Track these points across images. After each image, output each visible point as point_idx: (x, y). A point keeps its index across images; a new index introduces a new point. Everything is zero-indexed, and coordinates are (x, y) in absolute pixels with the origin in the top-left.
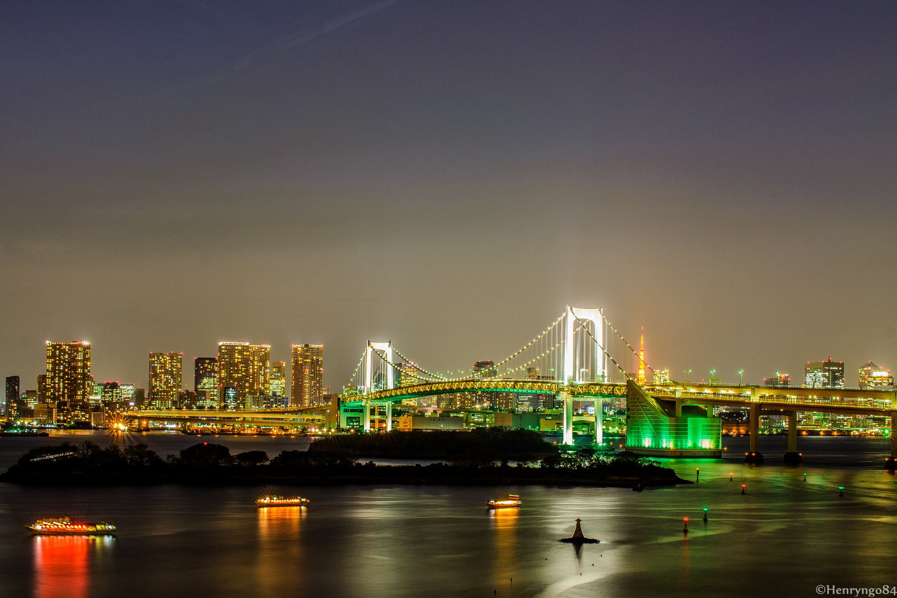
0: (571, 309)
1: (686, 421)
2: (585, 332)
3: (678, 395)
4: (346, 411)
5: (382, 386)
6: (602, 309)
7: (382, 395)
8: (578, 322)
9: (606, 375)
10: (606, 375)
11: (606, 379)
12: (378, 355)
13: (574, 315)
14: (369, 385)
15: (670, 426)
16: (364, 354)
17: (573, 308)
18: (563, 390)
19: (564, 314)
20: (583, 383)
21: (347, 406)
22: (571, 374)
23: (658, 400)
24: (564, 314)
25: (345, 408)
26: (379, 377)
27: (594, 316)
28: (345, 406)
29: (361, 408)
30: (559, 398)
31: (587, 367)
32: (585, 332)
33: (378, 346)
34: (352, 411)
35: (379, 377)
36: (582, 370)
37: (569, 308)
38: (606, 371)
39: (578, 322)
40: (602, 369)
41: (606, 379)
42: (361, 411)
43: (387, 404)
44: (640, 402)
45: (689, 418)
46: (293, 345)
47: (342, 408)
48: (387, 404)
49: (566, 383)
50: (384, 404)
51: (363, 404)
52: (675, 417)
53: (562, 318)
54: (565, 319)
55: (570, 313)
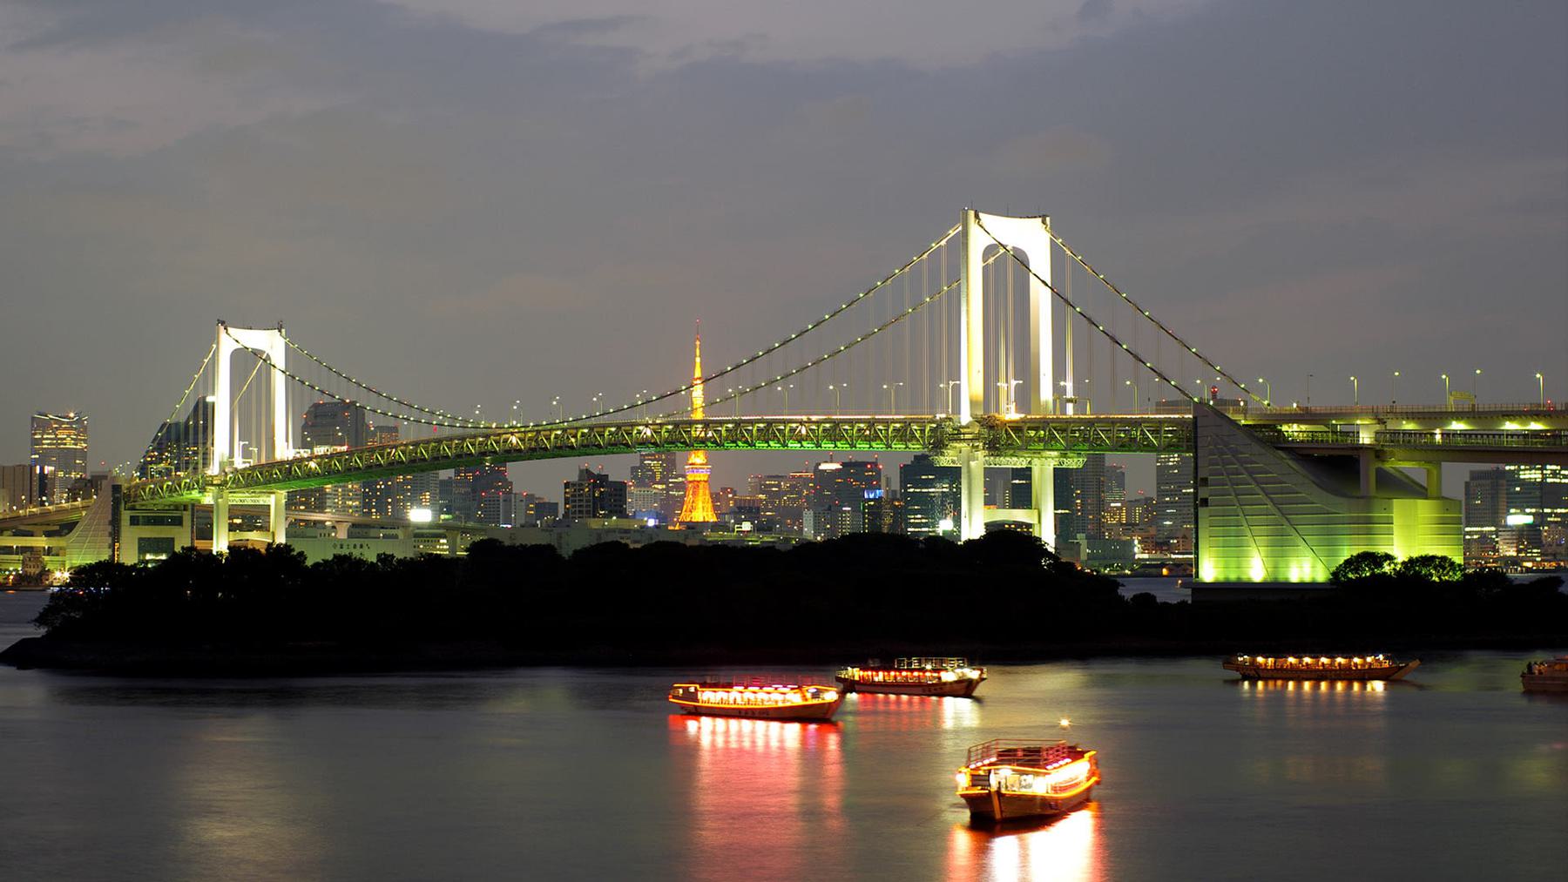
0: (977, 216)
1: (1389, 509)
4: (134, 521)
5: (256, 449)
6: (1048, 219)
7: (266, 474)
9: (1070, 394)
10: (1070, 394)
11: (1070, 407)
16: (206, 361)
17: (981, 215)
18: (957, 435)
19: (952, 233)
21: (138, 507)
25: (134, 513)
28: (133, 509)
29: (177, 514)
30: (946, 460)
37: (972, 213)
38: (1069, 385)
41: (1070, 407)
42: (178, 522)
43: (270, 500)
44: (1242, 462)
45: (1395, 500)
47: (126, 516)
48: (270, 500)
49: (965, 418)
50: (263, 500)
51: (207, 499)
52: (1362, 497)
53: (943, 243)
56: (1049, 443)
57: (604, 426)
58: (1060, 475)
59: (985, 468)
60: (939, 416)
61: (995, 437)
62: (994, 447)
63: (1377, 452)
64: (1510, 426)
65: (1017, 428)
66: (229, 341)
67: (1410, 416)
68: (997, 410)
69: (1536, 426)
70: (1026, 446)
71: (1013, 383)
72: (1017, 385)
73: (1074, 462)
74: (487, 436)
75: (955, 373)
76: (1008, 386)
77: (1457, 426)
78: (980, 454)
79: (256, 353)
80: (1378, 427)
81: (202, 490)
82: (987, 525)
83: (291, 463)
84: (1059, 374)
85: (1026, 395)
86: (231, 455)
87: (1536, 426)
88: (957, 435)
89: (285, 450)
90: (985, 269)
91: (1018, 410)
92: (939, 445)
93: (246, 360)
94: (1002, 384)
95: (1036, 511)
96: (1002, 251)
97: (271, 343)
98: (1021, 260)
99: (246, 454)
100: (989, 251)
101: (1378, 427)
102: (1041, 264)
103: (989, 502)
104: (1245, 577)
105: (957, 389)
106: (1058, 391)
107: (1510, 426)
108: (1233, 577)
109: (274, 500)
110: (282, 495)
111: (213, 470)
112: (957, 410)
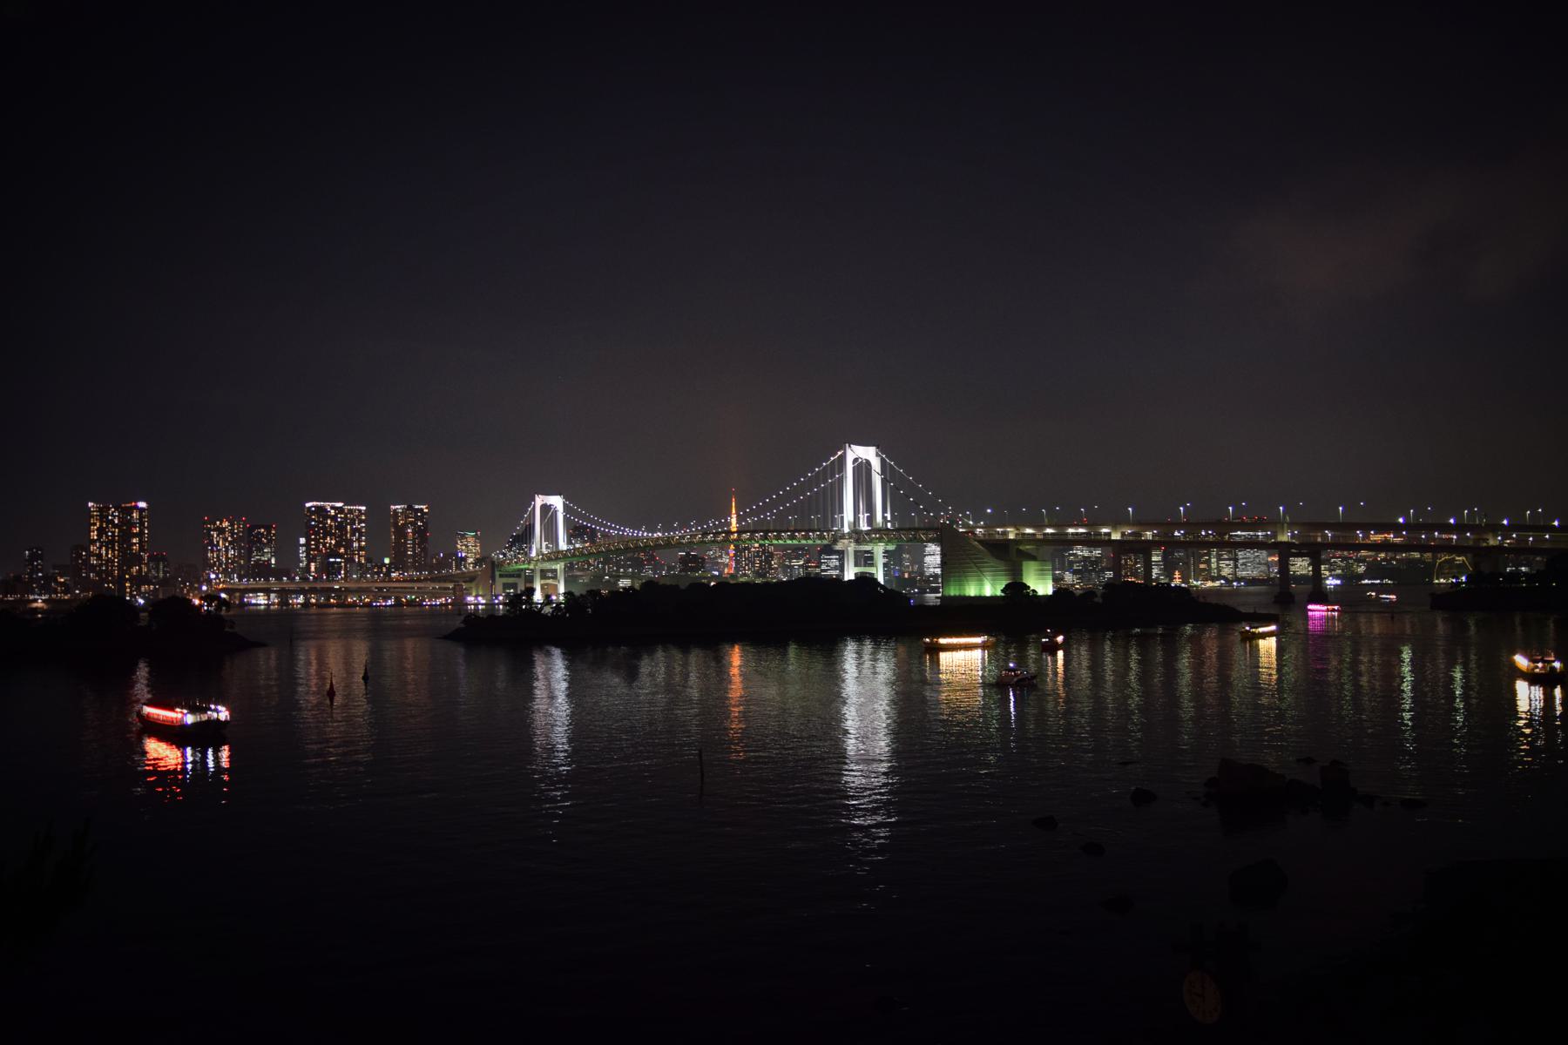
1: (1021, 565)
3: (1011, 536)
4: (501, 576)
9: (889, 519)
10: (889, 519)
15: (1005, 570)
18: (843, 536)
19: (839, 453)
20: (870, 528)
22: (852, 519)
24: (839, 453)
26: (550, 534)
34: (512, 576)
36: (866, 515)
37: (847, 445)
38: (888, 516)
42: (519, 576)
46: (393, 507)
47: (497, 573)
49: (846, 530)
55: (849, 452)
56: (880, 540)
57: (697, 535)
58: (886, 552)
59: (856, 552)
60: (835, 529)
61: (857, 536)
62: (858, 542)
64: (1071, 530)
65: (868, 533)
66: (539, 500)
67: (1029, 527)
68: (859, 526)
69: (1081, 530)
70: (871, 541)
71: (866, 515)
72: (868, 517)
73: (891, 547)
74: (647, 539)
75: (841, 511)
76: (863, 517)
77: (1049, 531)
78: (852, 544)
80: (1017, 532)
81: (529, 563)
82: (855, 574)
83: (566, 551)
84: (884, 511)
85: (871, 520)
86: (541, 548)
87: (1081, 530)
88: (843, 536)
89: (563, 546)
90: (854, 468)
91: (868, 526)
93: (546, 508)
94: (861, 516)
95: (875, 569)
96: (860, 460)
97: (557, 502)
98: (868, 463)
99: (547, 547)
100: (855, 460)
101: (1017, 532)
102: (876, 465)
103: (856, 565)
104: (962, 594)
105: (842, 517)
106: (884, 518)
107: (1071, 530)
108: (957, 594)
109: (559, 567)
110: (563, 564)
111: (533, 554)
112: (842, 526)
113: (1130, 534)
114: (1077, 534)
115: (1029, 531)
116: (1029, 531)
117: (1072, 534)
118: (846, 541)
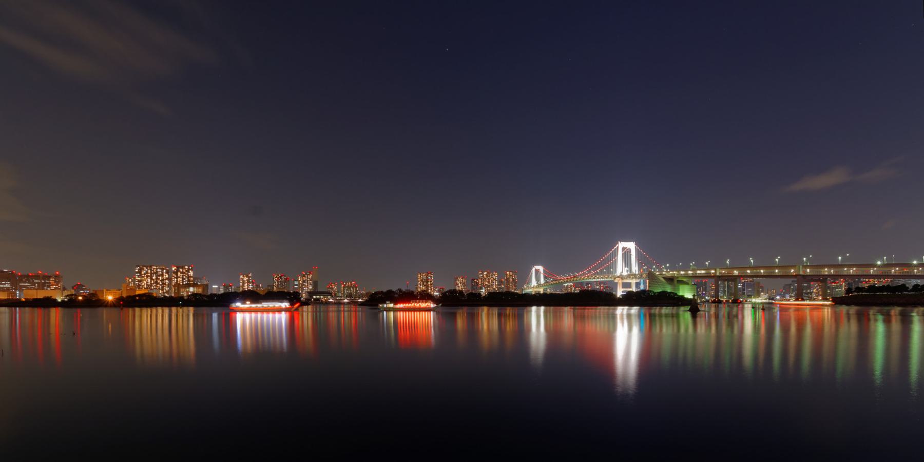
1: (679, 287)
2: (627, 253)
8: (623, 249)
12: (537, 271)
13: (622, 245)
14: (534, 283)
23: (664, 278)
24: (617, 245)
27: (631, 246)
30: (616, 281)
31: (628, 267)
32: (627, 253)
33: (537, 267)
35: (538, 279)
36: (626, 269)
39: (623, 249)
40: (635, 269)
49: (619, 275)
54: (618, 247)
61: (621, 277)
62: (622, 279)
63: (677, 278)
64: (698, 272)
67: (683, 271)
73: (638, 281)
79: (539, 270)
92: (615, 279)
107: (698, 272)
113: (725, 273)
114: (701, 273)
115: (682, 273)
116: (682, 273)
117: (698, 274)
118: (618, 279)
